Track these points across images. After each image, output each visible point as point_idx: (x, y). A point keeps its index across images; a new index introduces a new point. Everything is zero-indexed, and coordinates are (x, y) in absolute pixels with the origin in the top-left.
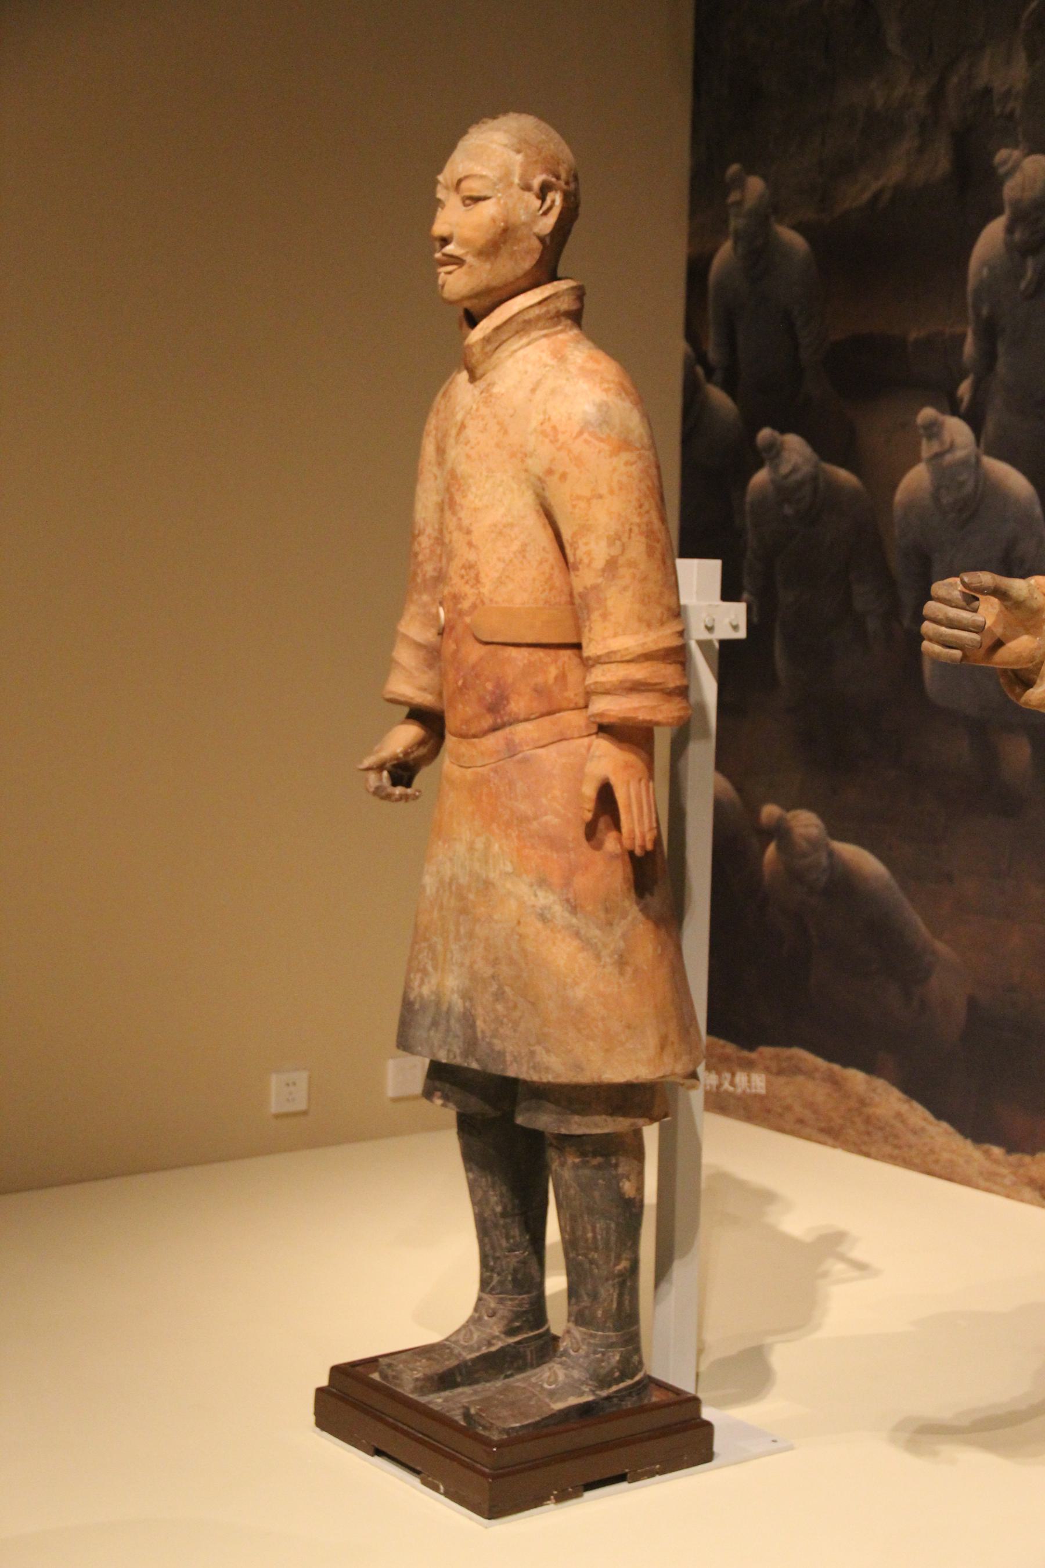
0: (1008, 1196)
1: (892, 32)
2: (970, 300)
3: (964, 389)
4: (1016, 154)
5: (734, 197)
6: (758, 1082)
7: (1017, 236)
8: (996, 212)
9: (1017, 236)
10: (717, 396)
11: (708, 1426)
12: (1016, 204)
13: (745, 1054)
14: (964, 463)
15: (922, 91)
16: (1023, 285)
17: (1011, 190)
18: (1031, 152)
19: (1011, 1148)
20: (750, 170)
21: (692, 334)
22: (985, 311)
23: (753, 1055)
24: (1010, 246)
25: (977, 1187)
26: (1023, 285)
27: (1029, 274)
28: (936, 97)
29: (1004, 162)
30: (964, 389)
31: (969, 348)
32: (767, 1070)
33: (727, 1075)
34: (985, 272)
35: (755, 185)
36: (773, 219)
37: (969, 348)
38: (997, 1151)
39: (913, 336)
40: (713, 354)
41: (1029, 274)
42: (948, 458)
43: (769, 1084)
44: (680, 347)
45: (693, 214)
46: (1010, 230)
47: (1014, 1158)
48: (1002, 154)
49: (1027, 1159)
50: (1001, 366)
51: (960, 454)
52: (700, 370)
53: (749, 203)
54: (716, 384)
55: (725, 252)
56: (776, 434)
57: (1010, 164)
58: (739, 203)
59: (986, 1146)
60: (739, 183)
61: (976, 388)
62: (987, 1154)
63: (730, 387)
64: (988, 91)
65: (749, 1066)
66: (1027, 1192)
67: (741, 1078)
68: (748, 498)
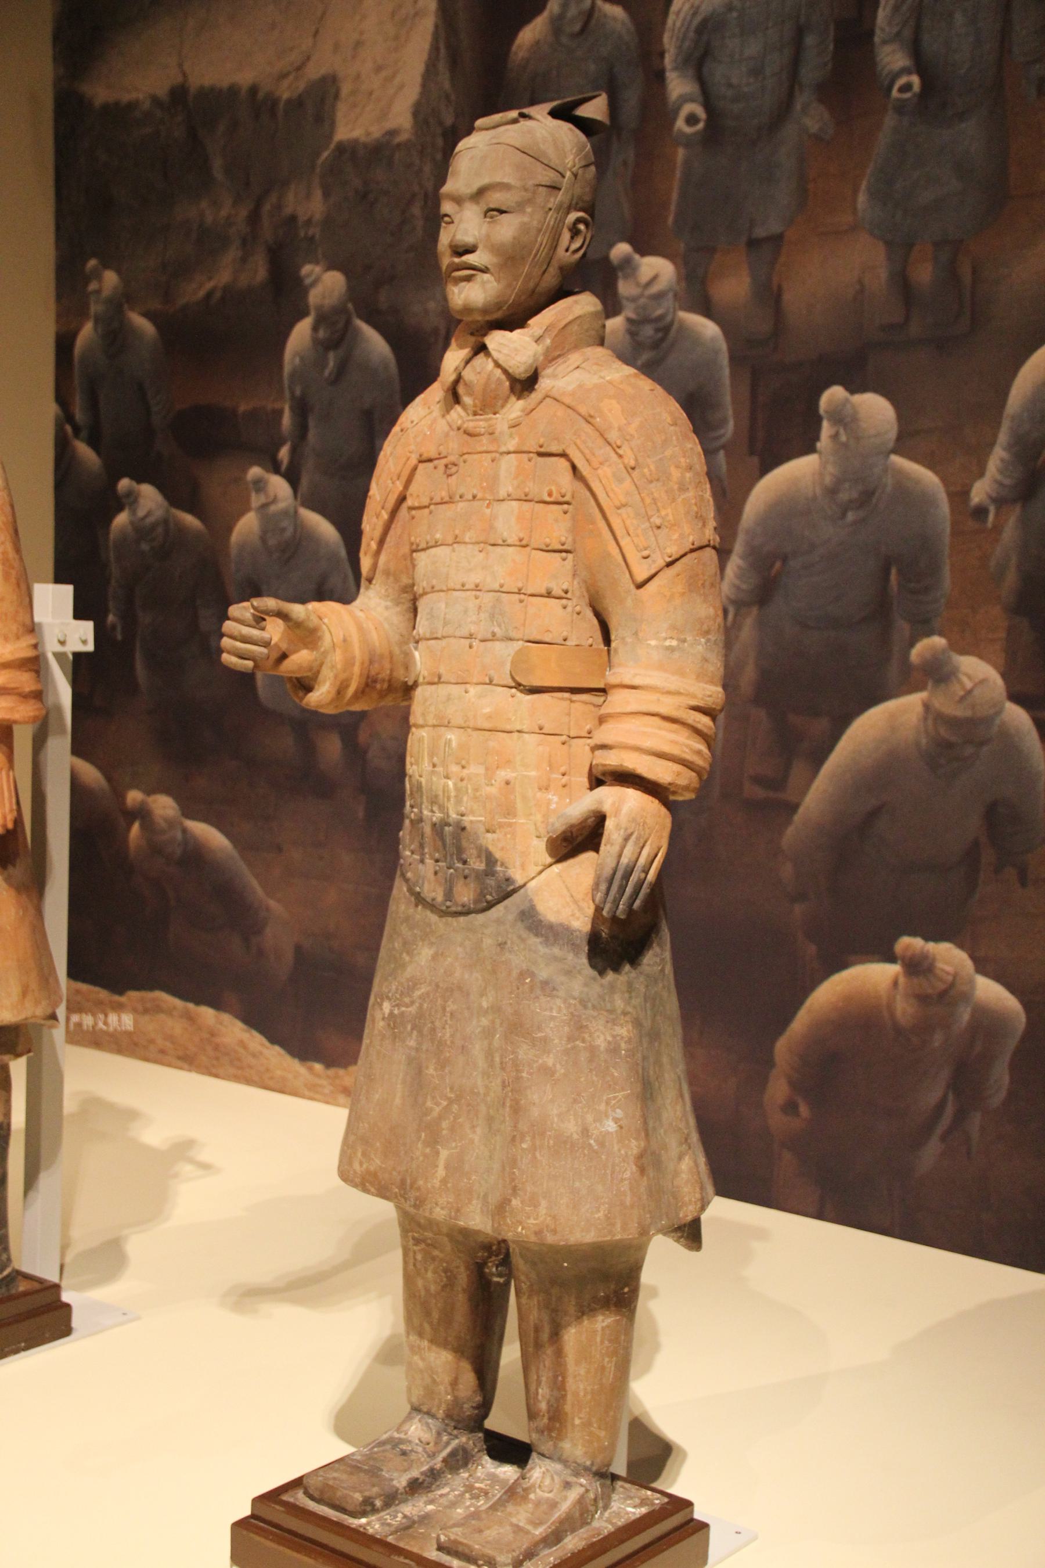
0: (327, 1103)
1: (217, 165)
2: (286, 382)
3: (284, 453)
4: (318, 269)
5: (93, 286)
6: (127, 1021)
7: (321, 334)
8: (303, 314)
10: (84, 451)
11: (67, 1307)
12: (319, 308)
13: (117, 998)
14: (285, 513)
15: (243, 213)
16: (327, 373)
17: (314, 297)
18: (330, 267)
19: (329, 1064)
20: (106, 266)
21: (62, 398)
22: (298, 392)
23: (123, 999)
24: (316, 341)
25: (303, 1096)
26: (327, 373)
27: (331, 364)
28: (254, 218)
29: (308, 275)
30: (284, 453)
32: (135, 1011)
33: (101, 1016)
34: (297, 360)
35: (111, 278)
36: (126, 306)
38: (318, 1067)
39: (242, 408)
40: (79, 416)
41: (331, 364)
42: (273, 508)
43: (136, 1022)
44: (51, 409)
45: (59, 297)
46: (315, 328)
47: (331, 1072)
49: (341, 1072)
50: (312, 435)
51: (281, 505)
52: (69, 429)
53: (106, 292)
54: (82, 440)
55: (87, 332)
56: (134, 484)
58: (98, 292)
59: (310, 1064)
60: (97, 275)
61: (293, 451)
62: (310, 1069)
63: (94, 442)
64: (293, 219)
65: (119, 1008)
67: (113, 1018)
68: (112, 536)
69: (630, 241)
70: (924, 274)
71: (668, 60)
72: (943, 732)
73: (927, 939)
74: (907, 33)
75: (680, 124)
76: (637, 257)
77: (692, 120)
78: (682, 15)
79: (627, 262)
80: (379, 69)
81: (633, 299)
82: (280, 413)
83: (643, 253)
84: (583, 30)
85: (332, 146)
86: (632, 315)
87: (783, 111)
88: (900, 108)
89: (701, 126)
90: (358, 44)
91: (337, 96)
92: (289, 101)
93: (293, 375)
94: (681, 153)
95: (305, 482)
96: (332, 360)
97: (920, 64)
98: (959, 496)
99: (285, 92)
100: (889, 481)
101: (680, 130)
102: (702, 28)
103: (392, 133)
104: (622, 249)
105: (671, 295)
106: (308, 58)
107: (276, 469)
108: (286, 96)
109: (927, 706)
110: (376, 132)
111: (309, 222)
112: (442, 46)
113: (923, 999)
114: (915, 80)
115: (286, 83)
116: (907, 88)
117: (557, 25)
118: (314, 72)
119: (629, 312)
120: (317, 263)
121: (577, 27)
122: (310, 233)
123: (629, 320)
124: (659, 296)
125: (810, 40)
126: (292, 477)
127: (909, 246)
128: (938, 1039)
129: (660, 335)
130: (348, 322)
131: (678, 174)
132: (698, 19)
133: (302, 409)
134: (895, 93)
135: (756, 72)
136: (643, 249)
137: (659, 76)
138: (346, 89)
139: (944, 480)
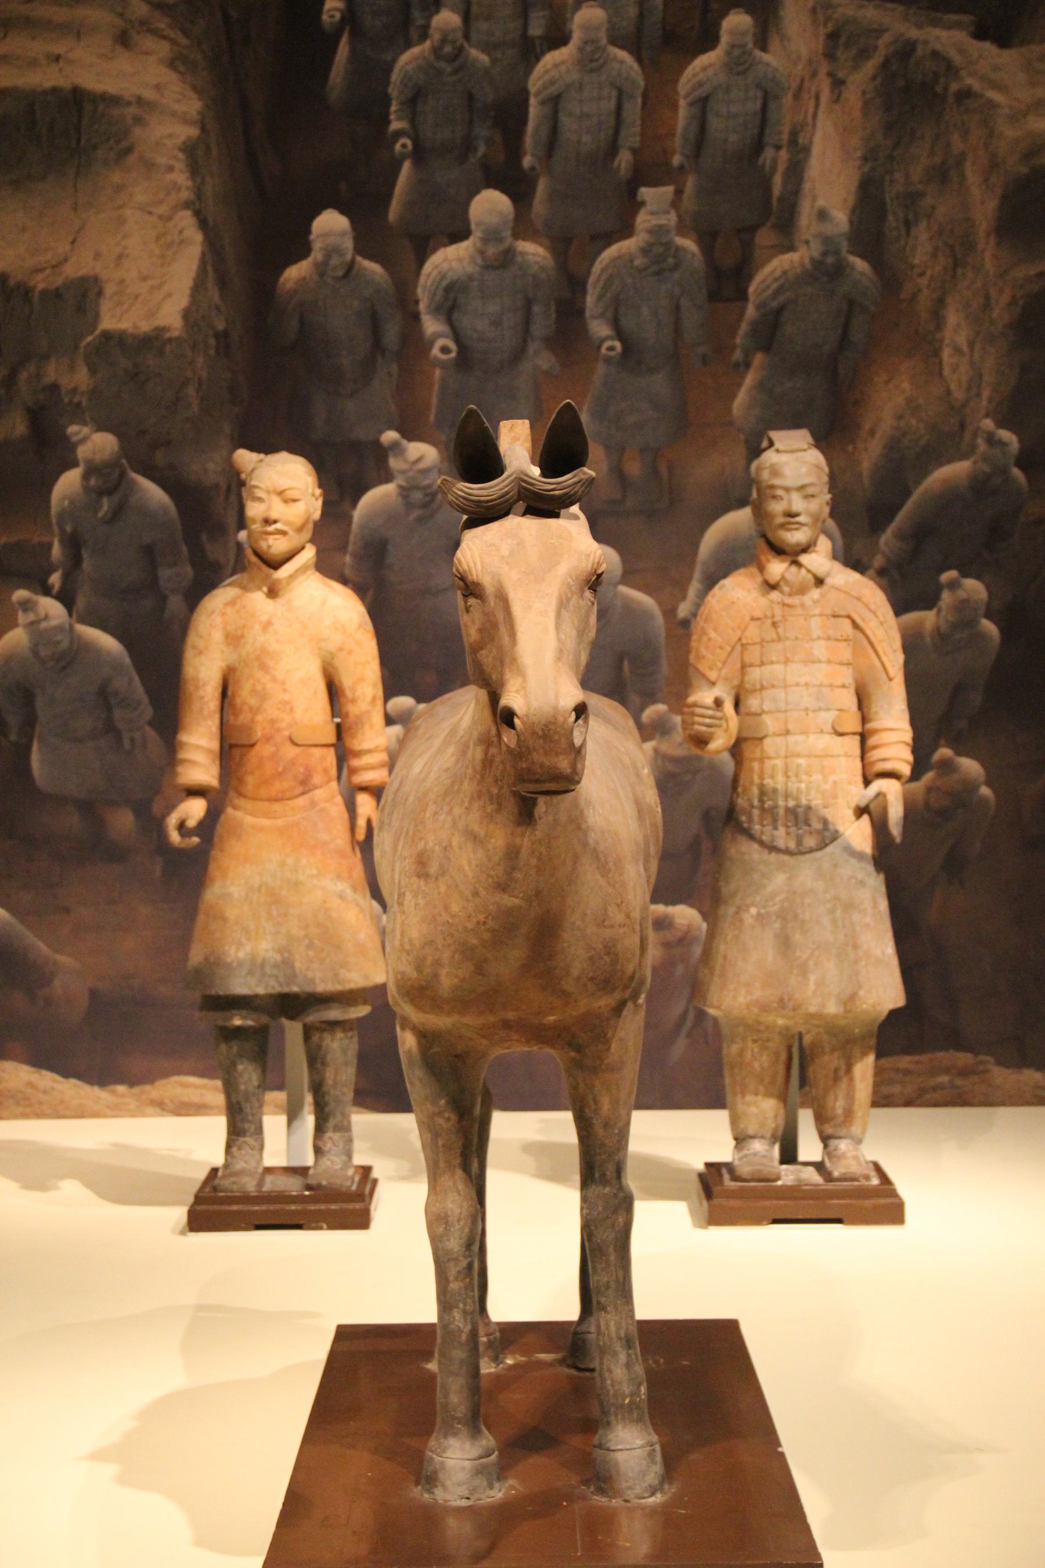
2: (54, 520)
3: (55, 579)
4: (86, 430)
9: (93, 482)
14: (60, 628)
16: (100, 514)
19: (132, 1084)
22: (68, 529)
24: (86, 489)
25: (105, 1116)
26: (100, 514)
27: (105, 507)
29: (77, 433)
30: (55, 579)
31: (56, 551)
34: (66, 503)
37: (56, 551)
38: (121, 1089)
41: (105, 507)
42: (44, 625)
46: (86, 477)
47: (136, 1090)
48: (72, 429)
49: (148, 1088)
50: (87, 565)
51: (54, 622)
57: (81, 436)
59: (112, 1087)
61: (66, 578)
62: (113, 1092)
64: (54, 387)
66: (150, 1110)
69: (398, 430)
70: (634, 468)
71: (422, 307)
72: (670, 767)
73: (667, 904)
74: (609, 315)
75: (435, 351)
76: (404, 442)
77: (445, 350)
78: (432, 278)
79: (395, 446)
80: (145, 279)
81: (404, 472)
82: (50, 546)
83: (410, 439)
84: (346, 275)
85: (98, 332)
86: (403, 483)
87: (518, 354)
88: (608, 361)
89: (453, 355)
90: (120, 257)
91: (100, 293)
92: (44, 292)
93: (61, 516)
94: (438, 373)
95: (81, 603)
96: (106, 505)
97: (620, 334)
98: (669, 613)
99: (40, 282)
100: (618, 602)
101: (435, 357)
102: (450, 288)
103: (161, 330)
104: (390, 436)
105: (436, 471)
106: (66, 260)
107: (47, 591)
108: (41, 286)
109: (656, 751)
110: (146, 327)
111: (74, 391)
112: (210, 268)
113: (666, 945)
114: (618, 345)
115: (40, 277)
116: (611, 349)
117: (322, 269)
118: (71, 271)
119: (400, 481)
120: (85, 424)
121: (340, 273)
122: (76, 399)
123: (400, 487)
124: (425, 472)
125: (536, 309)
126: (66, 598)
127: (622, 450)
128: (680, 970)
129: (427, 499)
130: (123, 475)
131: (436, 387)
132: (444, 283)
133: (74, 544)
134: (603, 350)
135: (497, 323)
136: (410, 434)
137: (416, 317)
138: (109, 289)
139: (660, 603)
